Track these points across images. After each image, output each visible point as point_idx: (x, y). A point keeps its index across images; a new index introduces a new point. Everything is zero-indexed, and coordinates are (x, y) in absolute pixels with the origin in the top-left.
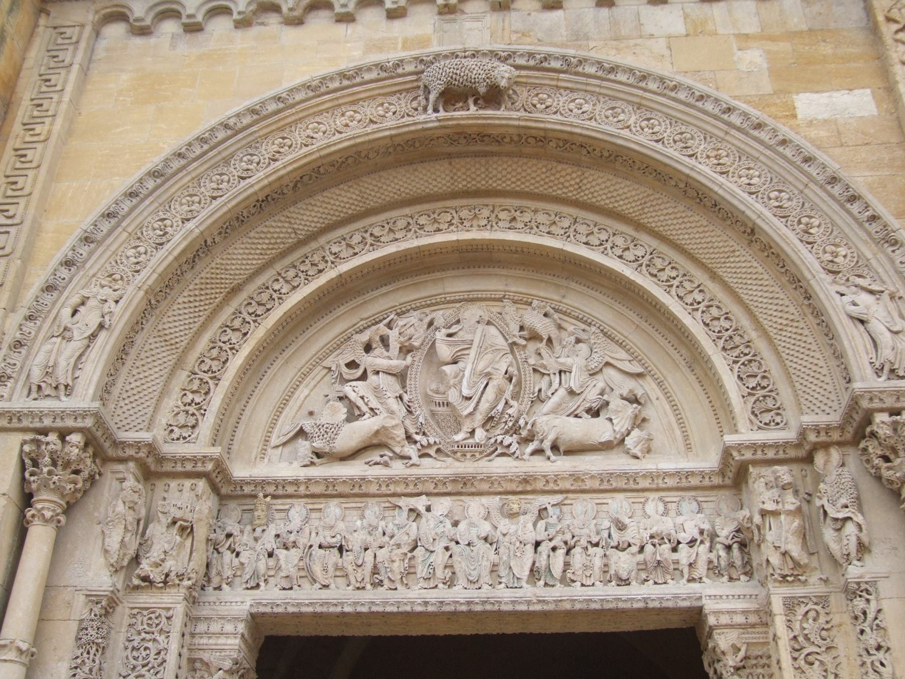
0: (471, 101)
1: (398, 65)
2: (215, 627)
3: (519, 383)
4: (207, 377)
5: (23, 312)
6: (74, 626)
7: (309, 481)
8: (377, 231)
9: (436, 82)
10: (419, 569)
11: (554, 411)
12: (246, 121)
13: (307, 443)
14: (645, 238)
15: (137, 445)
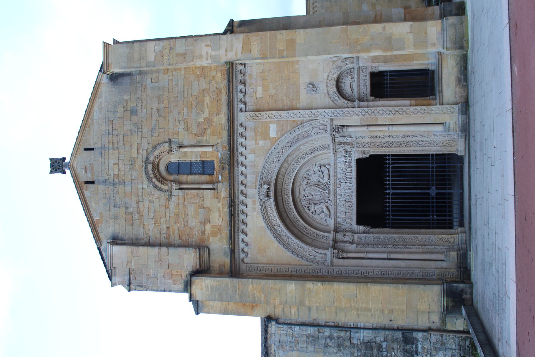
0: (269, 192)
1: (261, 206)
2: (359, 230)
3: (316, 185)
4: (317, 236)
5: (312, 264)
6: (361, 249)
7: (334, 218)
8: (289, 209)
9: (264, 199)
10: (349, 200)
11: (323, 179)
12: (272, 232)
13: (328, 219)
14: (293, 163)
15: (333, 243)
